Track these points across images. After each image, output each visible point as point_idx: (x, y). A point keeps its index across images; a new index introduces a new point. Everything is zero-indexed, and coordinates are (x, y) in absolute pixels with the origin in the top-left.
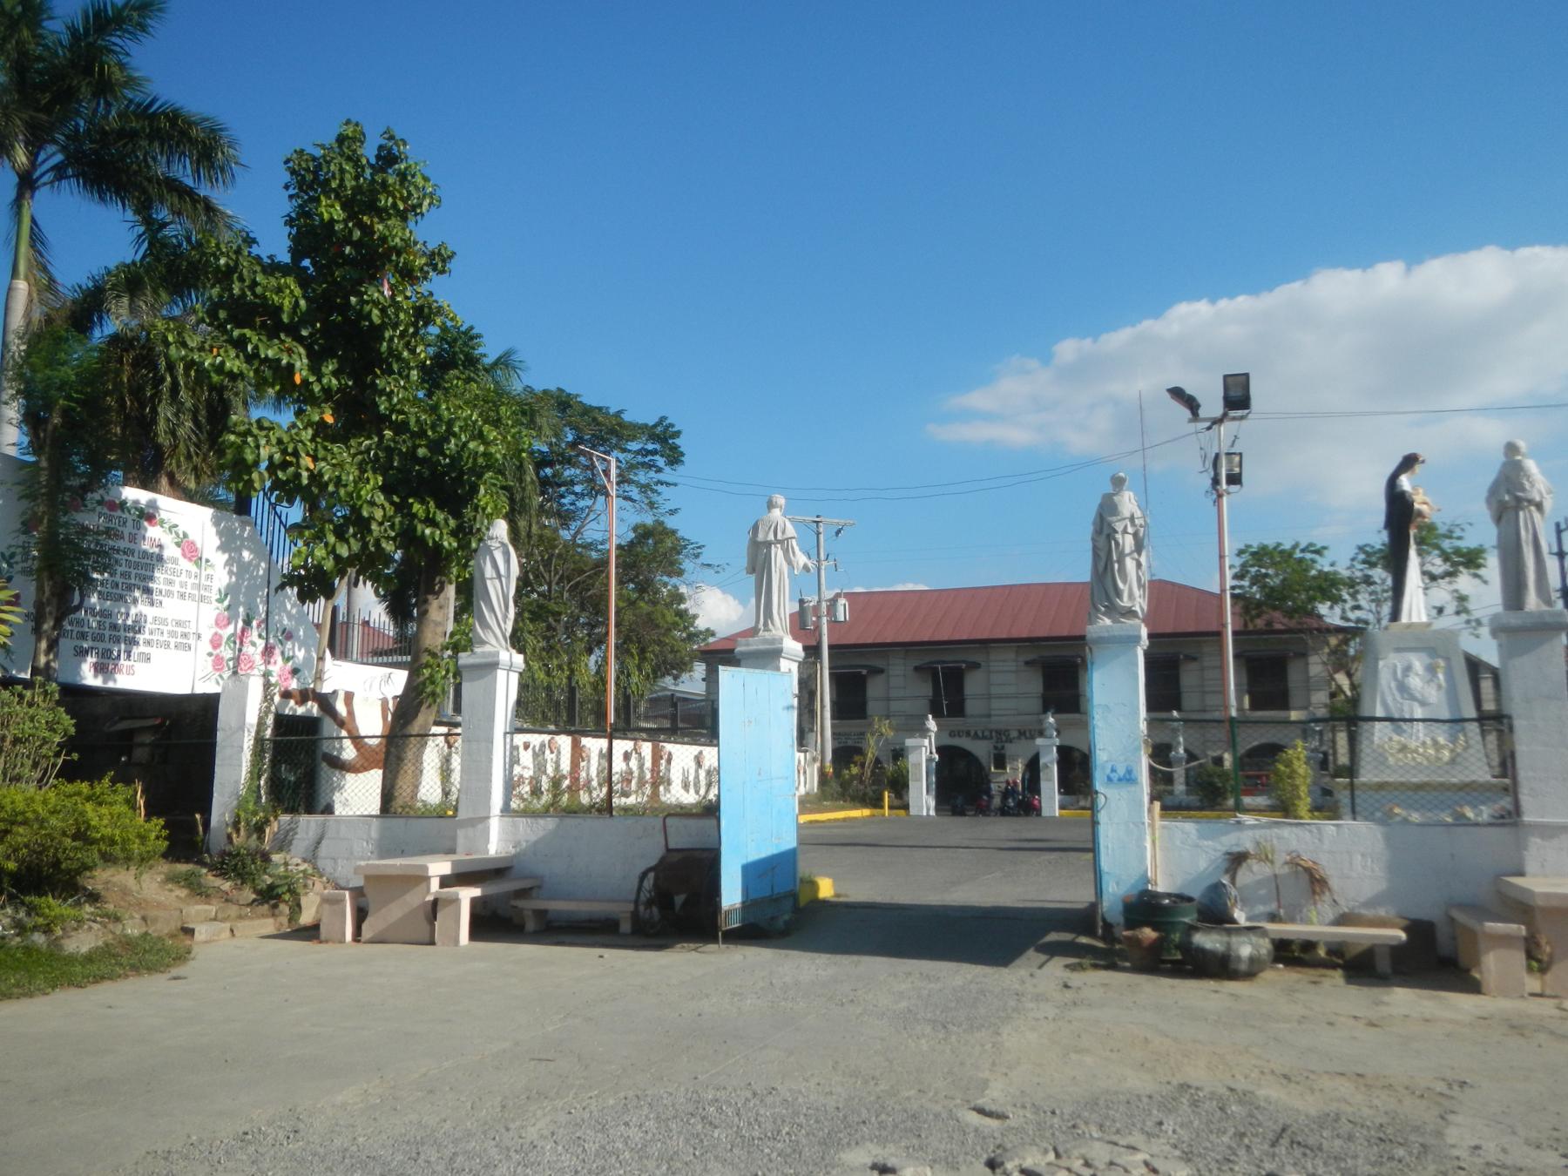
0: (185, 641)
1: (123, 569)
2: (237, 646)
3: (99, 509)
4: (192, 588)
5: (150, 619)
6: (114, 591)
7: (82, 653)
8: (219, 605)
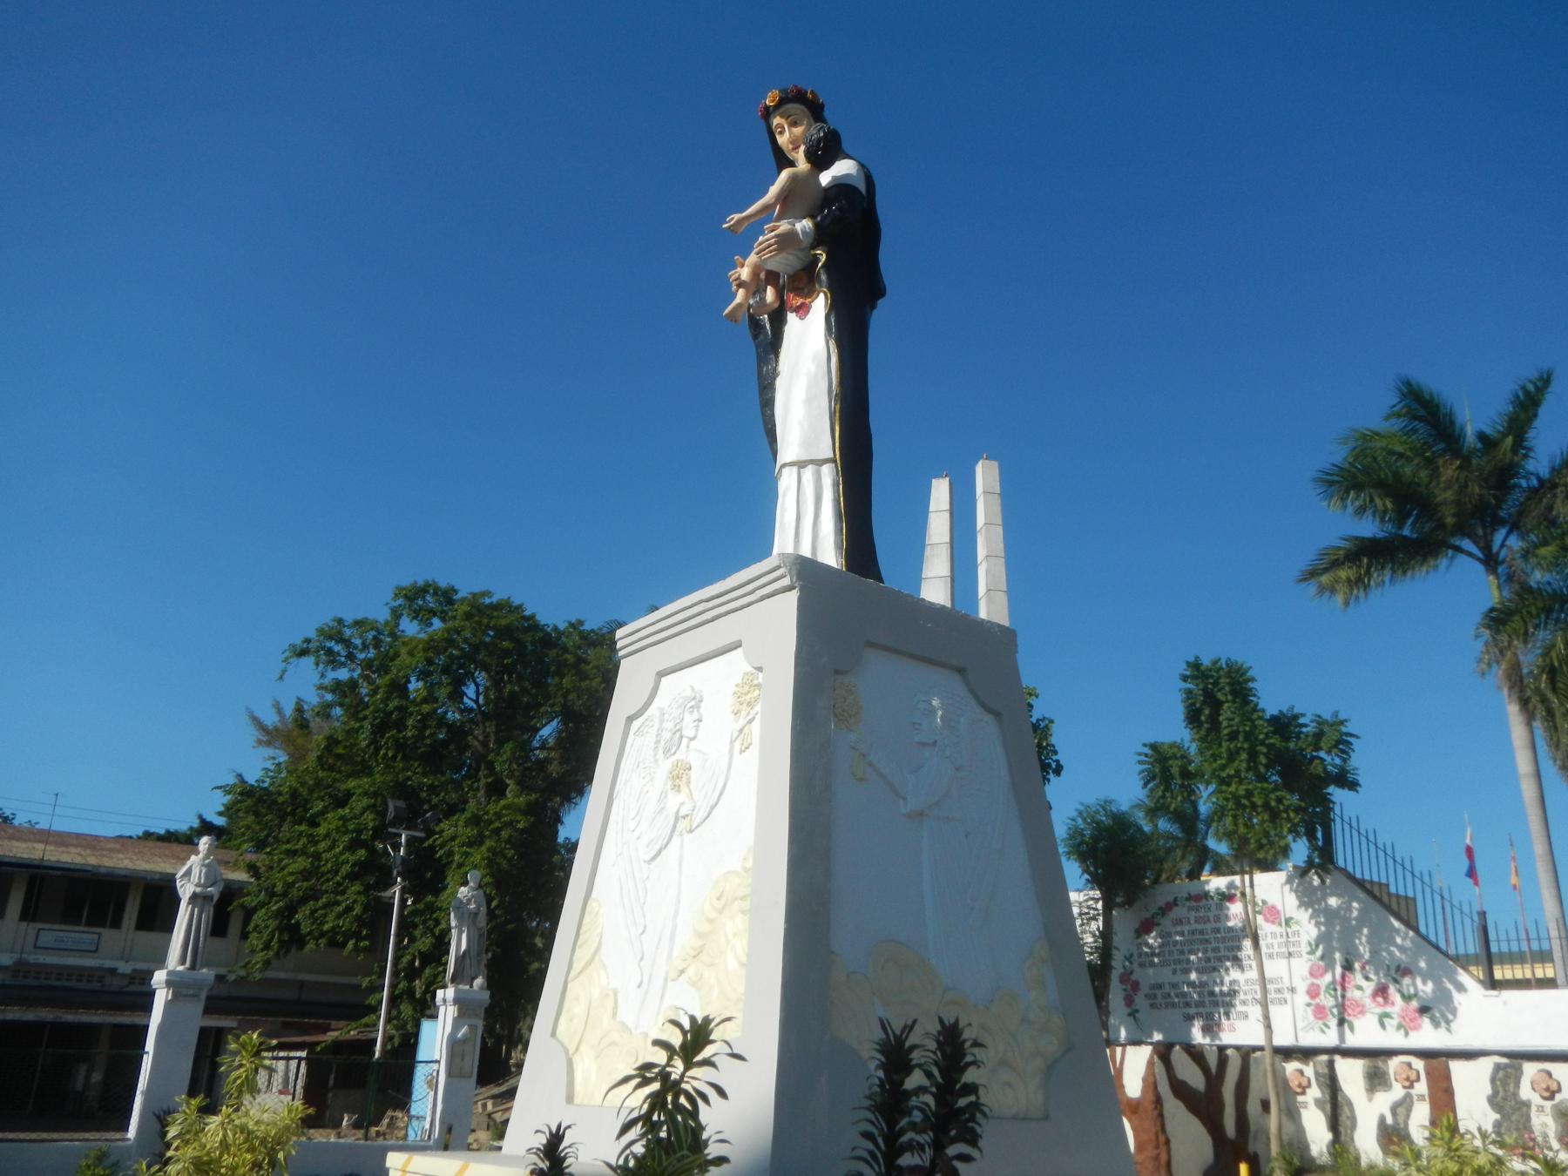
0: (1279, 996)
1: (1213, 945)
2: (1339, 993)
3: (1188, 904)
4: (1279, 948)
5: (1242, 983)
6: (1209, 964)
7: (1189, 1019)
8: (1312, 957)
